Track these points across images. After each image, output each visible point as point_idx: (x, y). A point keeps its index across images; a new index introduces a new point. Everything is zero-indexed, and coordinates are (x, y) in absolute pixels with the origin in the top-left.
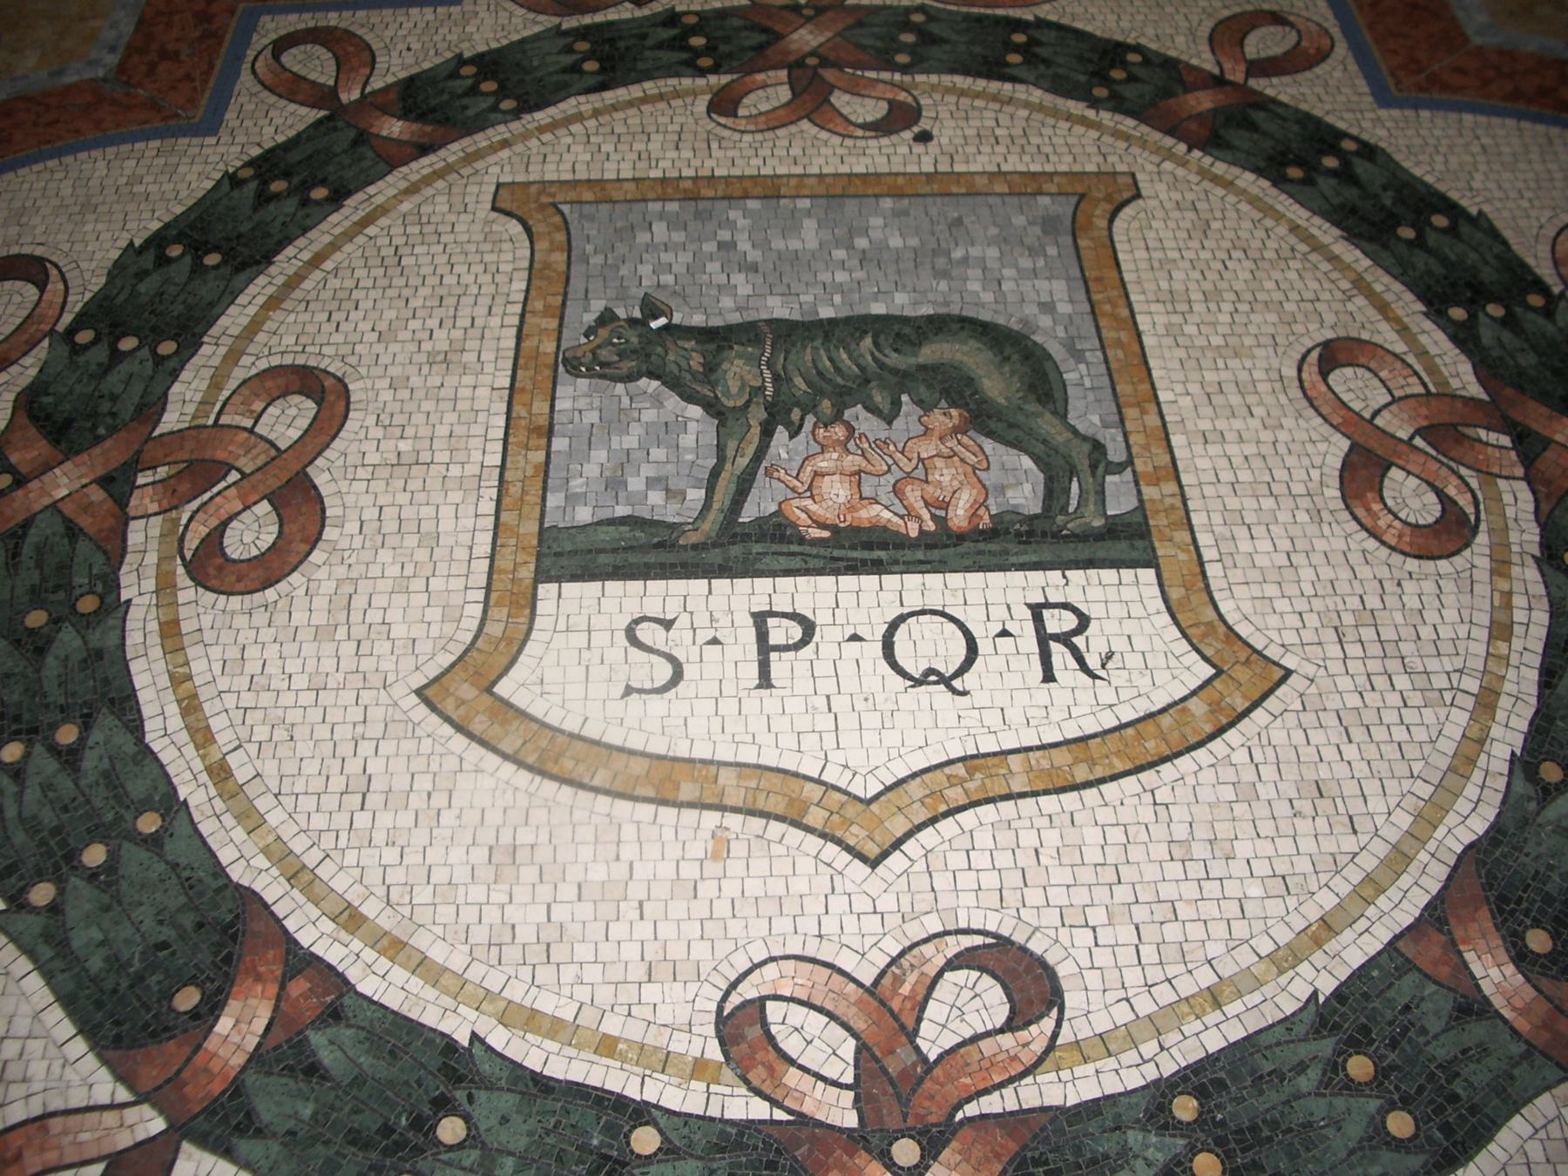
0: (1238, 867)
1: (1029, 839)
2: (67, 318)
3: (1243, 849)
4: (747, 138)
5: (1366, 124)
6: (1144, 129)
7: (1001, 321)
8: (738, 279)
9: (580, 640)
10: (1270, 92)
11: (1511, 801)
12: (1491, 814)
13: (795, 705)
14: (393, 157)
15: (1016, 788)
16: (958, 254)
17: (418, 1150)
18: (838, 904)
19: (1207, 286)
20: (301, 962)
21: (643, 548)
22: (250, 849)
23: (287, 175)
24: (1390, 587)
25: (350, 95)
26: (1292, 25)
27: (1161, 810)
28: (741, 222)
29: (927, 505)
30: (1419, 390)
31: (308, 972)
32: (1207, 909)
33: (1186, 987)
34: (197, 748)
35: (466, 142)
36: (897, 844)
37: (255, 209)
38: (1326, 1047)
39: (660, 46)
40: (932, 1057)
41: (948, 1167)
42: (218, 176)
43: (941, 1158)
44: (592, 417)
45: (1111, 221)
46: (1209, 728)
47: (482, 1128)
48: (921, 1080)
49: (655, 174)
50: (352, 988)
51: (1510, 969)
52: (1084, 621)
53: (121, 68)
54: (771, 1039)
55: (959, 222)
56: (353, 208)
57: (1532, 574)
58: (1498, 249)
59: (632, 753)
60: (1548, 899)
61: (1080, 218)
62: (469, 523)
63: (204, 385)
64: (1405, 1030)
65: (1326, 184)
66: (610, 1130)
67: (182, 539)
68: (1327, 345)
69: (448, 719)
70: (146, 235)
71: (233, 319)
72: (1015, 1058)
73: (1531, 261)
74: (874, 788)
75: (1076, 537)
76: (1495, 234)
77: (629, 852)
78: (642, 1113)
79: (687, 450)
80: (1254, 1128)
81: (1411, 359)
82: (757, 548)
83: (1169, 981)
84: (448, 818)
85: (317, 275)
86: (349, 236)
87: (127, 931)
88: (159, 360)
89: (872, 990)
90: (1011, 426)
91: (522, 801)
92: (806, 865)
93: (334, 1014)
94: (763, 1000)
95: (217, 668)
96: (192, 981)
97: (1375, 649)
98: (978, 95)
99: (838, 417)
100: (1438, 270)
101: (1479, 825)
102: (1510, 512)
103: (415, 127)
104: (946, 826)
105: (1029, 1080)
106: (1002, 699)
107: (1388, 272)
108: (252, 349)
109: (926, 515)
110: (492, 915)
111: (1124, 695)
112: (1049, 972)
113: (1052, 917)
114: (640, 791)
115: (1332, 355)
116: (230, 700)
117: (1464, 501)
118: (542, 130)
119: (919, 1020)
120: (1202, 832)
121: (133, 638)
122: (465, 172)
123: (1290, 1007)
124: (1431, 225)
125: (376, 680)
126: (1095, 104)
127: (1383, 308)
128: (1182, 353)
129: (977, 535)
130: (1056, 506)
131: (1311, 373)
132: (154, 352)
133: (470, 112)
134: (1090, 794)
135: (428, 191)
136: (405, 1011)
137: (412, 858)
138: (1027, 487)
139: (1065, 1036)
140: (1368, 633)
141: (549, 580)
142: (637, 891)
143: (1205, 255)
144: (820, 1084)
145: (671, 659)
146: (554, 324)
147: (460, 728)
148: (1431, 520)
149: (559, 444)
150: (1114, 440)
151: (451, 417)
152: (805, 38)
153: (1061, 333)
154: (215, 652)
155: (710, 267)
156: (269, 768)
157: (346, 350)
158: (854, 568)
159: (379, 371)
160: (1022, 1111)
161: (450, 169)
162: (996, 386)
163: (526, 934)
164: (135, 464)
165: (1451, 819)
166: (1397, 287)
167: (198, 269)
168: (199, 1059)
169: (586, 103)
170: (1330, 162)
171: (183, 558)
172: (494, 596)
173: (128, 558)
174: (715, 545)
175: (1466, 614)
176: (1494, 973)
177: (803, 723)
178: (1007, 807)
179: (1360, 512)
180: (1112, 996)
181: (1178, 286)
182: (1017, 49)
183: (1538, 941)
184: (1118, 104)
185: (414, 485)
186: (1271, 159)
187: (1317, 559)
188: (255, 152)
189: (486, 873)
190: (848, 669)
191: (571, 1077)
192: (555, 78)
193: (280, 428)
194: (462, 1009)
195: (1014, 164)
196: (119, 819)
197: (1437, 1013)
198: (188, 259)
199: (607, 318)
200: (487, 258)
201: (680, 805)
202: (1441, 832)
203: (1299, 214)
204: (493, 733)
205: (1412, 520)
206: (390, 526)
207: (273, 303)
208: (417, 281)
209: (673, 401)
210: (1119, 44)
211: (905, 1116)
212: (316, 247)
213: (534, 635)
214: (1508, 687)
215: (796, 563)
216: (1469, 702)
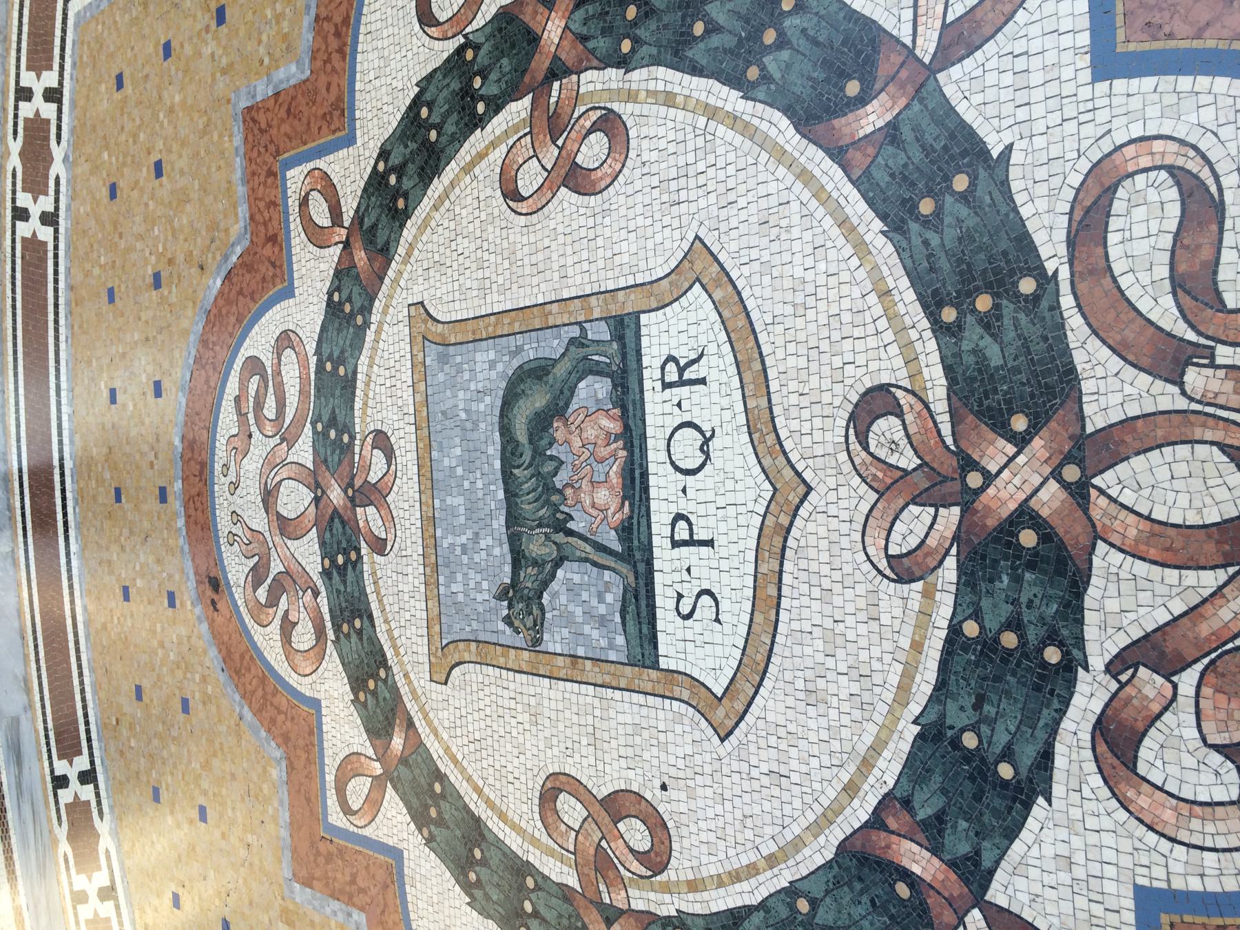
0: (809, 275)
1: (794, 399)
3: (799, 272)
4: (399, 533)
5: (367, 155)
6: (380, 295)
7: (501, 393)
8: (483, 544)
9: (690, 645)
10: (352, 213)
13: (723, 527)
14: (416, 744)
16: (463, 415)
17: (983, 760)
18: (832, 510)
19: (474, 266)
20: (876, 821)
21: (638, 607)
22: (815, 846)
23: (427, 807)
24: (645, 170)
25: (377, 768)
26: (307, 194)
27: (777, 320)
28: (450, 539)
29: (608, 444)
30: (529, 137)
31: (883, 815)
32: (833, 294)
33: (878, 310)
34: (758, 874)
35: (405, 699)
36: (798, 474)
37: (448, 828)
38: (914, 227)
39: (344, 582)
40: (919, 462)
41: (981, 457)
42: (427, 849)
43: (977, 459)
44: (565, 632)
45: (438, 322)
46: (730, 288)
47: (967, 722)
48: (933, 469)
49: (422, 587)
50: (891, 791)
51: (869, 108)
52: (671, 359)
53: (362, 909)
54: (909, 553)
55: (444, 413)
56: (445, 766)
57: (636, 75)
58: (439, 75)
59: (751, 620)
60: (827, 80)
62: (627, 706)
63: (552, 860)
64: (905, 178)
65: (407, 184)
67: (641, 877)
68: (505, 196)
69: (737, 724)
70: (463, 894)
71: (513, 842)
73: (445, 55)
74: (767, 486)
75: (624, 356)
76: (431, 76)
77: (807, 626)
78: (955, 630)
79: (582, 579)
80: (961, 273)
81: (511, 142)
82: (636, 543)
84: (792, 728)
85: (486, 790)
86: (463, 771)
88: (538, 887)
89: (881, 495)
90: (562, 392)
91: (780, 684)
92: (811, 527)
93: (907, 803)
94: (888, 557)
95: (713, 859)
97: (683, 181)
98: (366, 395)
99: (560, 492)
100: (455, 116)
101: (784, 122)
102: (599, 87)
103: (397, 729)
104: (788, 445)
105: (932, 406)
106: (716, 409)
108: (530, 830)
109: (614, 446)
110: (845, 707)
111: (712, 338)
112: (869, 391)
113: (838, 388)
114: (773, 618)
115: (511, 194)
116: (731, 852)
117: (594, 115)
118: (397, 654)
119: (898, 468)
120: (789, 296)
121: (698, 909)
122: (424, 701)
123: (890, 248)
124: (427, 119)
125: (717, 765)
126: (367, 324)
127: (481, 156)
128: (515, 286)
129: (624, 416)
130: (607, 370)
131: (523, 207)
132: (533, 891)
133: (388, 696)
134: (769, 361)
135: (436, 722)
136: (903, 762)
137: (815, 750)
138: (597, 386)
139: (905, 383)
140: (673, 185)
141: (658, 662)
142: (828, 623)
143: (455, 265)
145: (699, 596)
146: (512, 652)
147: (742, 718)
148: (606, 139)
149: (581, 652)
150: (567, 332)
151: (567, 714)
152: (336, 495)
153: (506, 358)
154: (705, 860)
155: (477, 560)
156: (769, 831)
157: (530, 774)
158: (646, 489)
159: (542, 755)
160: (950, 411)
161: (422, 709)
162: (537, 400)
163: (855, 688)
164: (599, 905)
165: (781, 140)
166: (467, 145)
167: (484, 862)
169: (381, 628)
170: (393, 180)
171: (651, 877)
172: (667, 694)
173: (653, 910)
174: (635, 566)
175: (661, 122)
176: (872, 118)
177: (733, 524)
180: (883, 355)
181: (475, 285)
182: (335, 369)
183: (853, 88)
184: (367, 309)
185: (606, 736)
186: (393, 218)
187: (631, 214)
188: (412, 826)
189: (822, 708)
190: (702, 497)
191: (936, 669)
192: (365, 645)
193: (576, 815)
194: (900, 728)
195: (407, 376)
197: (895, 156)
198: (477, 869)
199: (508, 620)
200: (475, 688)
201: (780, 596)
202: (788, 148)
203: (426, 204)
204: (744, 699)
205: (606, 151)
206: (630, 752)
207: (502, 816)
208: (489, 732)
209: (554, 586)
210: (328, 305)
211: (953, 479)
212: (470, 790)
213: (688, 672)
214: (703, 97)
215: (644, 521)
216: (712, 124)
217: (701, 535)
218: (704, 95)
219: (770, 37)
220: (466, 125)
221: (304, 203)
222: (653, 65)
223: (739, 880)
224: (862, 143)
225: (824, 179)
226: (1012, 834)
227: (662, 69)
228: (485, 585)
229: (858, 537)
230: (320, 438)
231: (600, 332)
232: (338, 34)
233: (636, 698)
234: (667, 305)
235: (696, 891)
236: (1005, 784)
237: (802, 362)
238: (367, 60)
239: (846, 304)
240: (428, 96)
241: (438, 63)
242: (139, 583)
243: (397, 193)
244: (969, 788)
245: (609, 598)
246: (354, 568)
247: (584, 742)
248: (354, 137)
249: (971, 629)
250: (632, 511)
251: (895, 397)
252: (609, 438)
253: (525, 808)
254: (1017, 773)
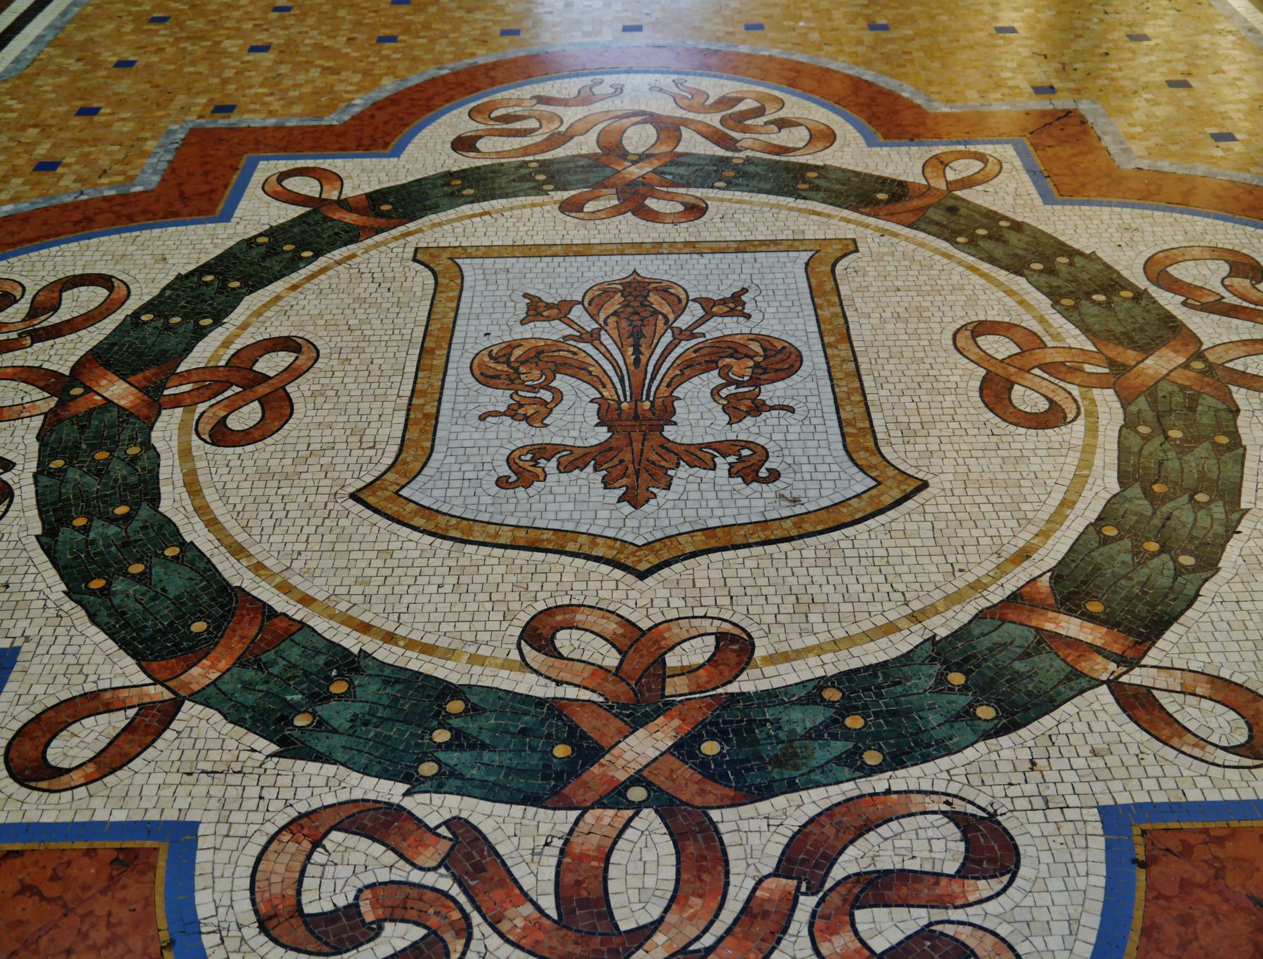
115: (981, 328)
152: (636, 171)
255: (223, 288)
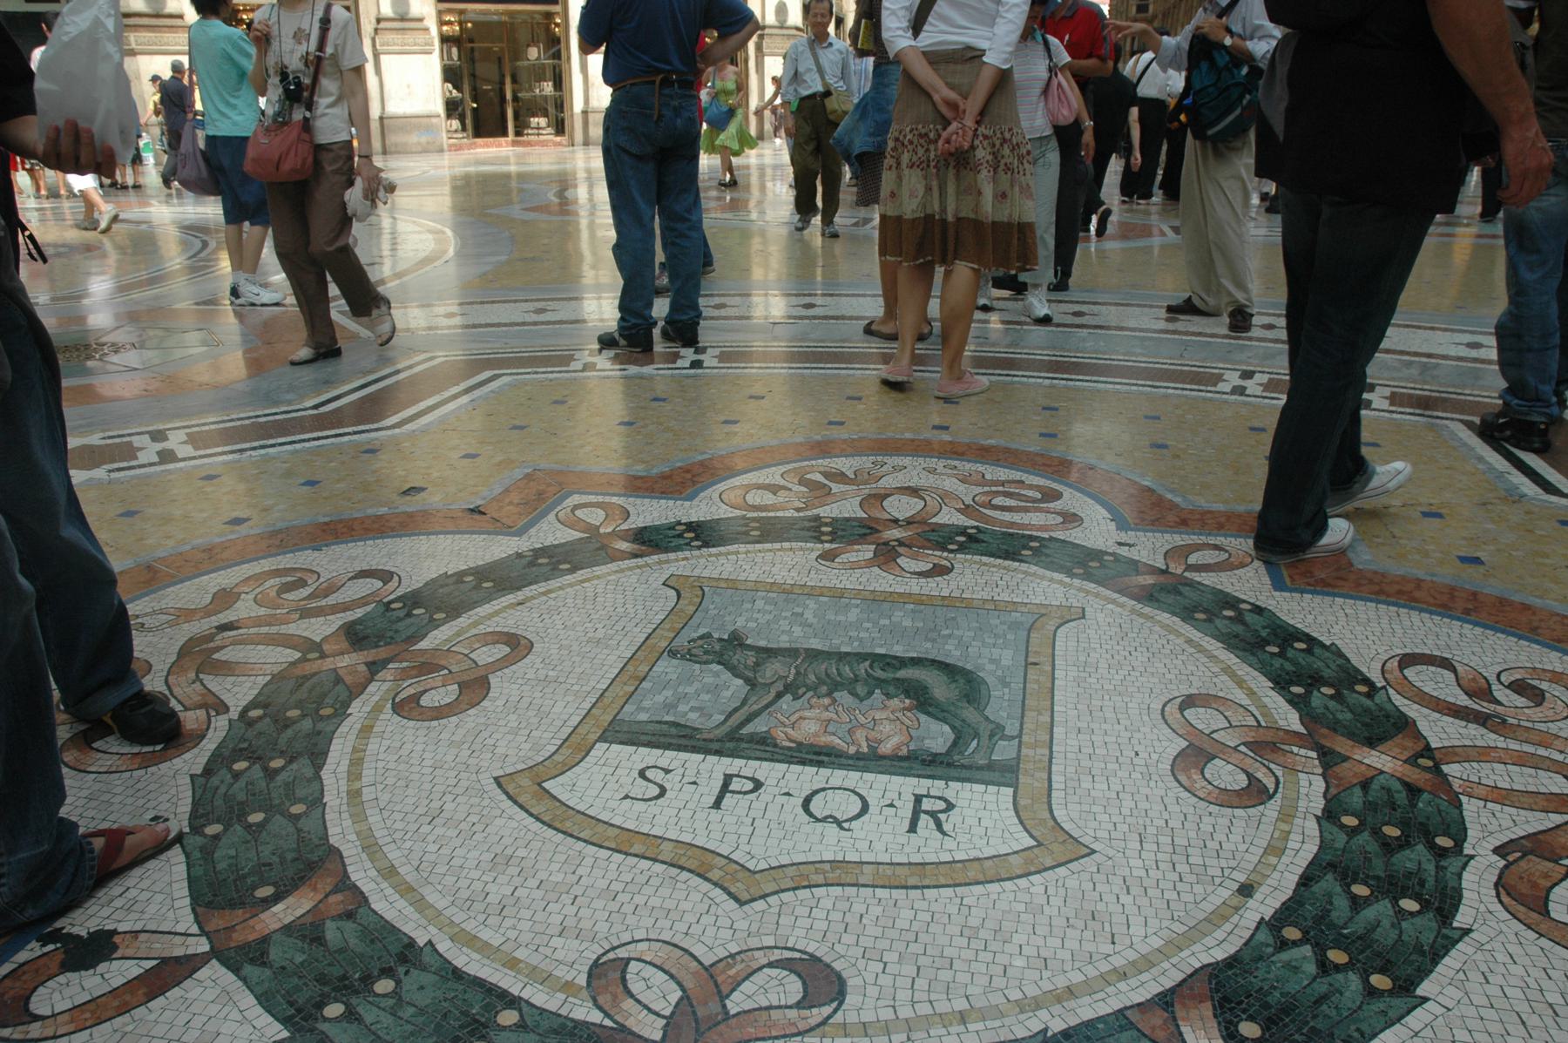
1: (859, 908)
2: (392, 597)
6: (1101, 589)
7: (960, 664)
11: (1253, 943)
12: (1232, 950)
15: (861, 881)
17: (357, 992)
18: (705, 920)
20: (344, 884)
21: (671, 736)
27: (965, 910)
29: (867, 739)
33: (942, 1007)
36: (764, 897)
40: (732, 1012)
45: (1058, 627)
46: (1019, 872)
52: (950, 806)
54: (624, 980)
57: (1312, 827)
58: (1340, 661)
60: (1266, 1006)
61: (1038, 624)
62: (571, 711)
66: (487, 1008)
69: (507, 793)
72: (794, 1024)
78: (513, 1002)
81: (1252, 708)
82: (746, 745)
83: (931, 1002)
85: (544, 598)
86: (571, 585)
87: (252, 854)
90: (943, 711)
93: (350, 915)
94: (629, 960)
95: (383, 749)
96: (274, 884)
98: (994, 566)
99: (829, 694)
101: (1219, 954)
103: (636, 547)
107: (1250, 666)
109: (864, 744)
110: (478, 886)
112: (842, 982)
114: (606, 844)
115: (1189, 702)
119: (733, 990)
120: (989, 924)
125: (474, 769)
126: (1072, 575)
127: (1240, 683)
131: (1172, 709)
138: (941, 740)
139: (839, 1017)
142: (577, 890)
144: (645, 1012)
147: (510, 797)
148: (1237, 788)
149: (644, 684)
150: (1012, 724)
152: (895, 533)
155: (781, 622)
156: (385, 797)
162: (941, 689)
165: (1197, 948)
166: (1256, 673)
168: (251, 922)
175: (1248, 840)
178: (851, 891)
179: (1183, 778)
182: (1031, 548)
184: (1088, 577)
191: (478, 975)
196: (283, 803)
199: (707, 636)
202: (1183, 954)
203: (1195, 635)
209: (726, 675)
210: (1101, 551)
215: (768, 755)
217: (728, 800)
218: (1275, 884)
219: (1337, 956)
220: (1280, 676)
221: (1217, 547)
222: (1322, 841)
223: (352, 764)
224: (1173, 1028)
225: (1133, 982)
226: (266, 1000)
227: (1315, 849)
228: (752, 625)
229: (666, 936)
230: (963, 531)
231: (1004, 751)
232: (1400, 592)
233: (576, 720)
234: (1017, 812)
235: (361, 731)
236: (320, 1006)
237: (900, 924)
238: (1366, 610)
239: (963, 978)
240: (1317, 651)
241: (1355, 661)
242: (862, 407)
243: (1211, 615)
244: (336, 971)
245: (693, 716)
246: (815, 538)
247: (551, 673)
248: (1282, 590)
249: (508, 1017)
250: (783, 748)
251: (824, 1005)
252: (874, 745)
253: (511, 622)
254: (326, 1019)
255: (477, 587)
